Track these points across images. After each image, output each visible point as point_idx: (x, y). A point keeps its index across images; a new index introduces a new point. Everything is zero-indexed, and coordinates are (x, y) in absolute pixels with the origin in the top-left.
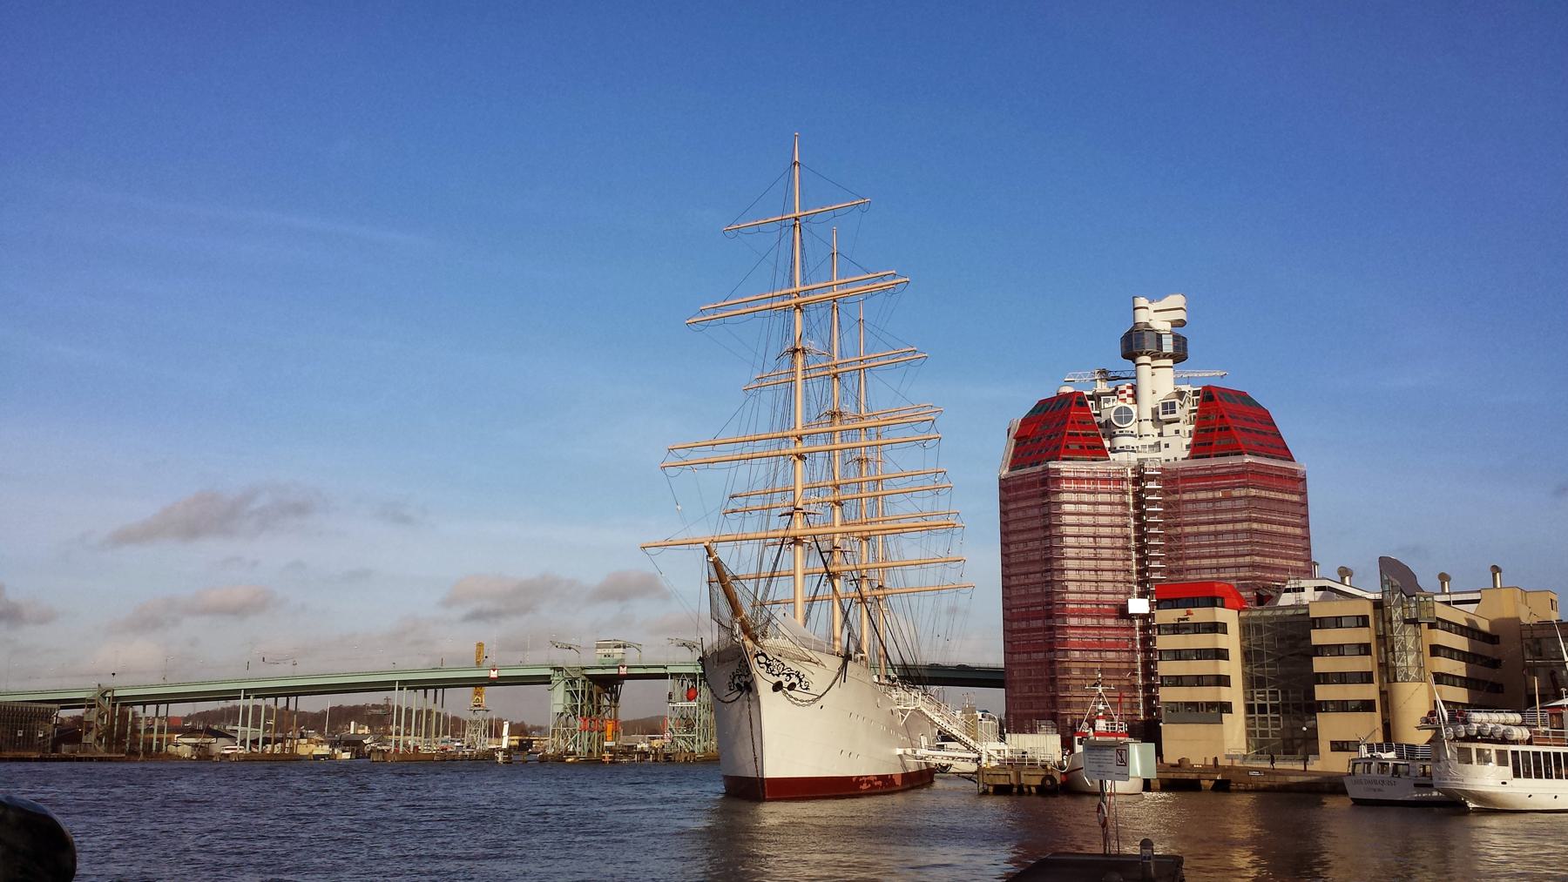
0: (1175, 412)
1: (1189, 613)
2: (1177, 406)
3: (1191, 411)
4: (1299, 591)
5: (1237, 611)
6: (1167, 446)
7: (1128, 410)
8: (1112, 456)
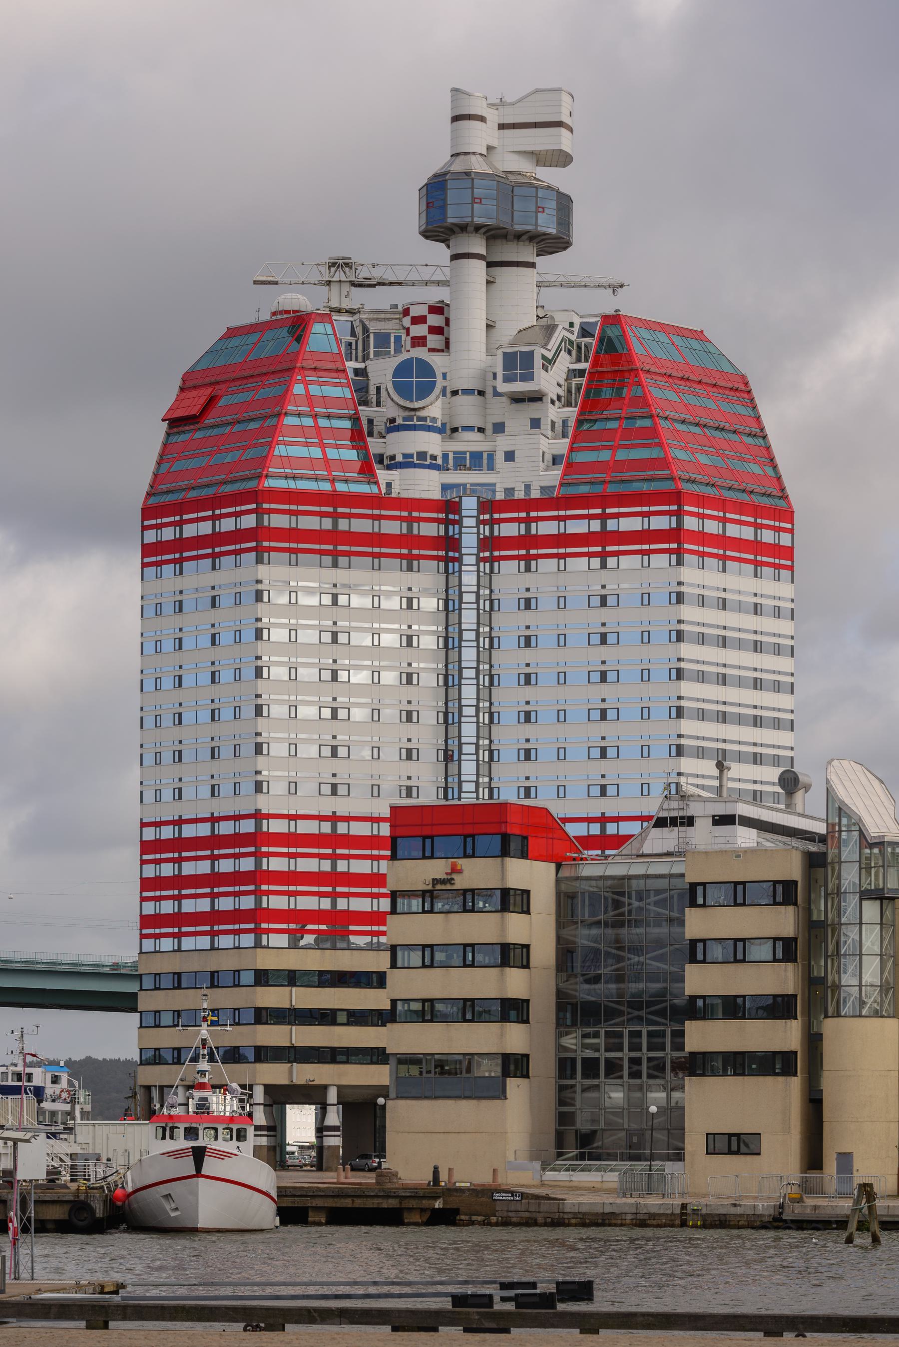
0: (529, 377)
1: (455, 870)
2: (538, 362)
3: (572, 374)
4: (682, 824)
5: (553, 866)
6: (510, 456)
7: (426, 369)
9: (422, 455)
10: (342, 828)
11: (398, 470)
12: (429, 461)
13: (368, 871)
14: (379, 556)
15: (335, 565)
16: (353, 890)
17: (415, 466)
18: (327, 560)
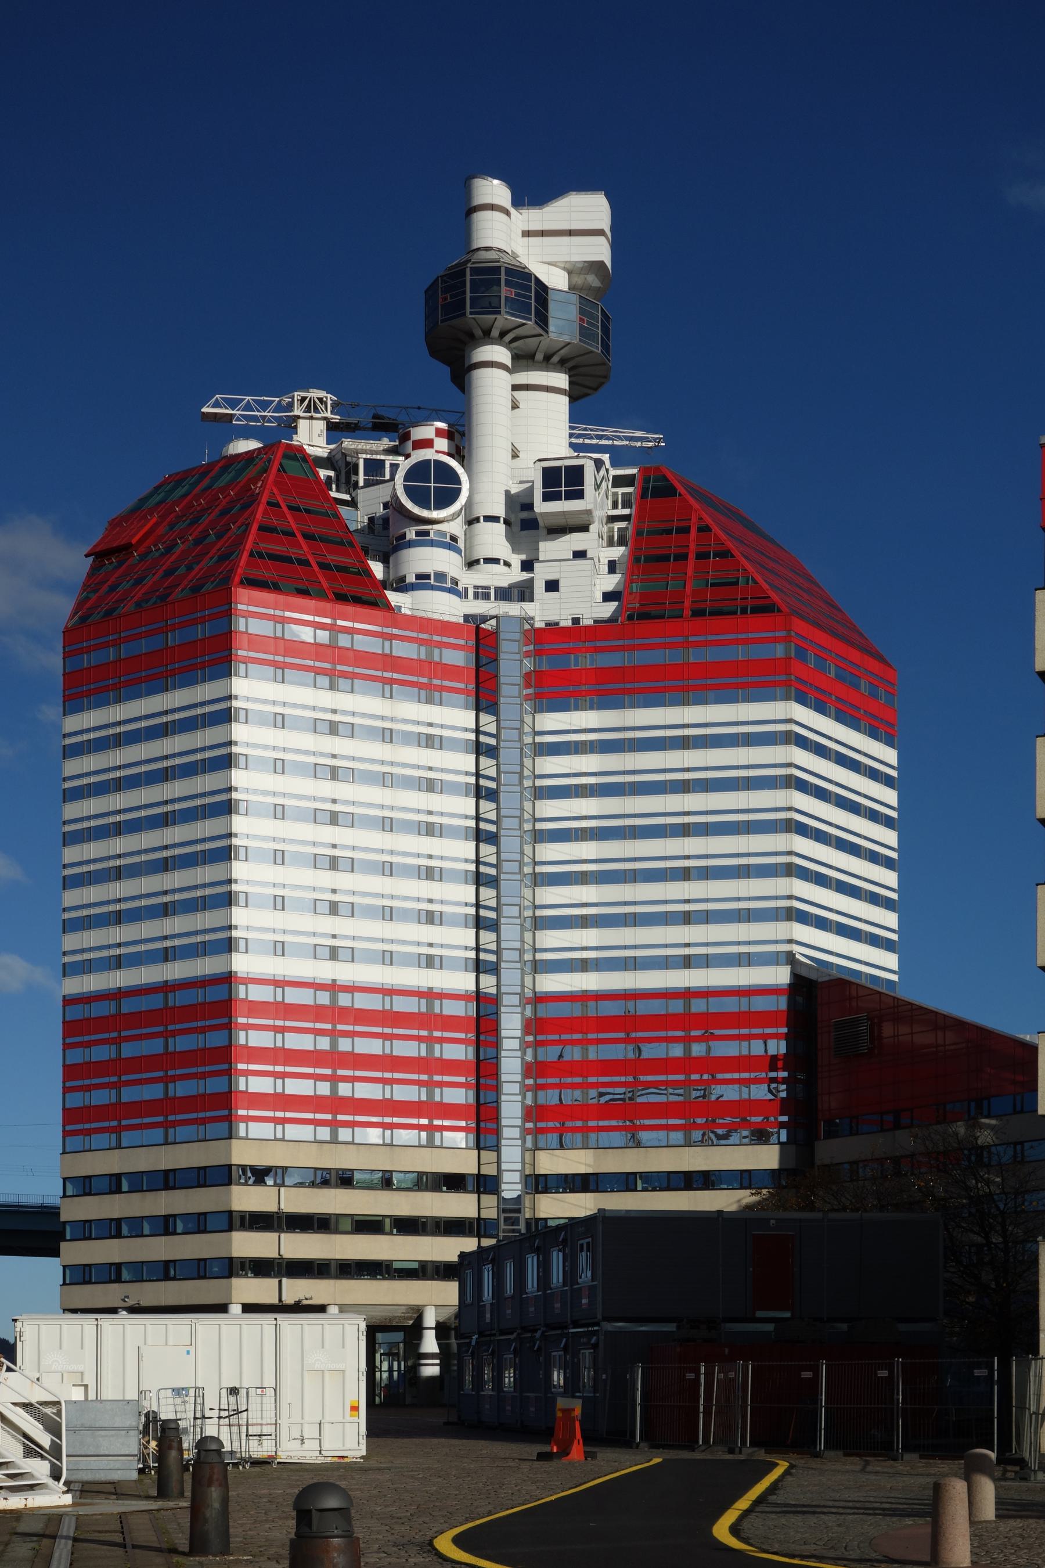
6: (552, 586)
8: (394, 597)
9: (441, 576)
10: (344, 1000)
11: (410, 593)
12: (449, 585)
13: (378, 1051)
14: (391, 682)
16: (358, 1073)
17: (432, 588)
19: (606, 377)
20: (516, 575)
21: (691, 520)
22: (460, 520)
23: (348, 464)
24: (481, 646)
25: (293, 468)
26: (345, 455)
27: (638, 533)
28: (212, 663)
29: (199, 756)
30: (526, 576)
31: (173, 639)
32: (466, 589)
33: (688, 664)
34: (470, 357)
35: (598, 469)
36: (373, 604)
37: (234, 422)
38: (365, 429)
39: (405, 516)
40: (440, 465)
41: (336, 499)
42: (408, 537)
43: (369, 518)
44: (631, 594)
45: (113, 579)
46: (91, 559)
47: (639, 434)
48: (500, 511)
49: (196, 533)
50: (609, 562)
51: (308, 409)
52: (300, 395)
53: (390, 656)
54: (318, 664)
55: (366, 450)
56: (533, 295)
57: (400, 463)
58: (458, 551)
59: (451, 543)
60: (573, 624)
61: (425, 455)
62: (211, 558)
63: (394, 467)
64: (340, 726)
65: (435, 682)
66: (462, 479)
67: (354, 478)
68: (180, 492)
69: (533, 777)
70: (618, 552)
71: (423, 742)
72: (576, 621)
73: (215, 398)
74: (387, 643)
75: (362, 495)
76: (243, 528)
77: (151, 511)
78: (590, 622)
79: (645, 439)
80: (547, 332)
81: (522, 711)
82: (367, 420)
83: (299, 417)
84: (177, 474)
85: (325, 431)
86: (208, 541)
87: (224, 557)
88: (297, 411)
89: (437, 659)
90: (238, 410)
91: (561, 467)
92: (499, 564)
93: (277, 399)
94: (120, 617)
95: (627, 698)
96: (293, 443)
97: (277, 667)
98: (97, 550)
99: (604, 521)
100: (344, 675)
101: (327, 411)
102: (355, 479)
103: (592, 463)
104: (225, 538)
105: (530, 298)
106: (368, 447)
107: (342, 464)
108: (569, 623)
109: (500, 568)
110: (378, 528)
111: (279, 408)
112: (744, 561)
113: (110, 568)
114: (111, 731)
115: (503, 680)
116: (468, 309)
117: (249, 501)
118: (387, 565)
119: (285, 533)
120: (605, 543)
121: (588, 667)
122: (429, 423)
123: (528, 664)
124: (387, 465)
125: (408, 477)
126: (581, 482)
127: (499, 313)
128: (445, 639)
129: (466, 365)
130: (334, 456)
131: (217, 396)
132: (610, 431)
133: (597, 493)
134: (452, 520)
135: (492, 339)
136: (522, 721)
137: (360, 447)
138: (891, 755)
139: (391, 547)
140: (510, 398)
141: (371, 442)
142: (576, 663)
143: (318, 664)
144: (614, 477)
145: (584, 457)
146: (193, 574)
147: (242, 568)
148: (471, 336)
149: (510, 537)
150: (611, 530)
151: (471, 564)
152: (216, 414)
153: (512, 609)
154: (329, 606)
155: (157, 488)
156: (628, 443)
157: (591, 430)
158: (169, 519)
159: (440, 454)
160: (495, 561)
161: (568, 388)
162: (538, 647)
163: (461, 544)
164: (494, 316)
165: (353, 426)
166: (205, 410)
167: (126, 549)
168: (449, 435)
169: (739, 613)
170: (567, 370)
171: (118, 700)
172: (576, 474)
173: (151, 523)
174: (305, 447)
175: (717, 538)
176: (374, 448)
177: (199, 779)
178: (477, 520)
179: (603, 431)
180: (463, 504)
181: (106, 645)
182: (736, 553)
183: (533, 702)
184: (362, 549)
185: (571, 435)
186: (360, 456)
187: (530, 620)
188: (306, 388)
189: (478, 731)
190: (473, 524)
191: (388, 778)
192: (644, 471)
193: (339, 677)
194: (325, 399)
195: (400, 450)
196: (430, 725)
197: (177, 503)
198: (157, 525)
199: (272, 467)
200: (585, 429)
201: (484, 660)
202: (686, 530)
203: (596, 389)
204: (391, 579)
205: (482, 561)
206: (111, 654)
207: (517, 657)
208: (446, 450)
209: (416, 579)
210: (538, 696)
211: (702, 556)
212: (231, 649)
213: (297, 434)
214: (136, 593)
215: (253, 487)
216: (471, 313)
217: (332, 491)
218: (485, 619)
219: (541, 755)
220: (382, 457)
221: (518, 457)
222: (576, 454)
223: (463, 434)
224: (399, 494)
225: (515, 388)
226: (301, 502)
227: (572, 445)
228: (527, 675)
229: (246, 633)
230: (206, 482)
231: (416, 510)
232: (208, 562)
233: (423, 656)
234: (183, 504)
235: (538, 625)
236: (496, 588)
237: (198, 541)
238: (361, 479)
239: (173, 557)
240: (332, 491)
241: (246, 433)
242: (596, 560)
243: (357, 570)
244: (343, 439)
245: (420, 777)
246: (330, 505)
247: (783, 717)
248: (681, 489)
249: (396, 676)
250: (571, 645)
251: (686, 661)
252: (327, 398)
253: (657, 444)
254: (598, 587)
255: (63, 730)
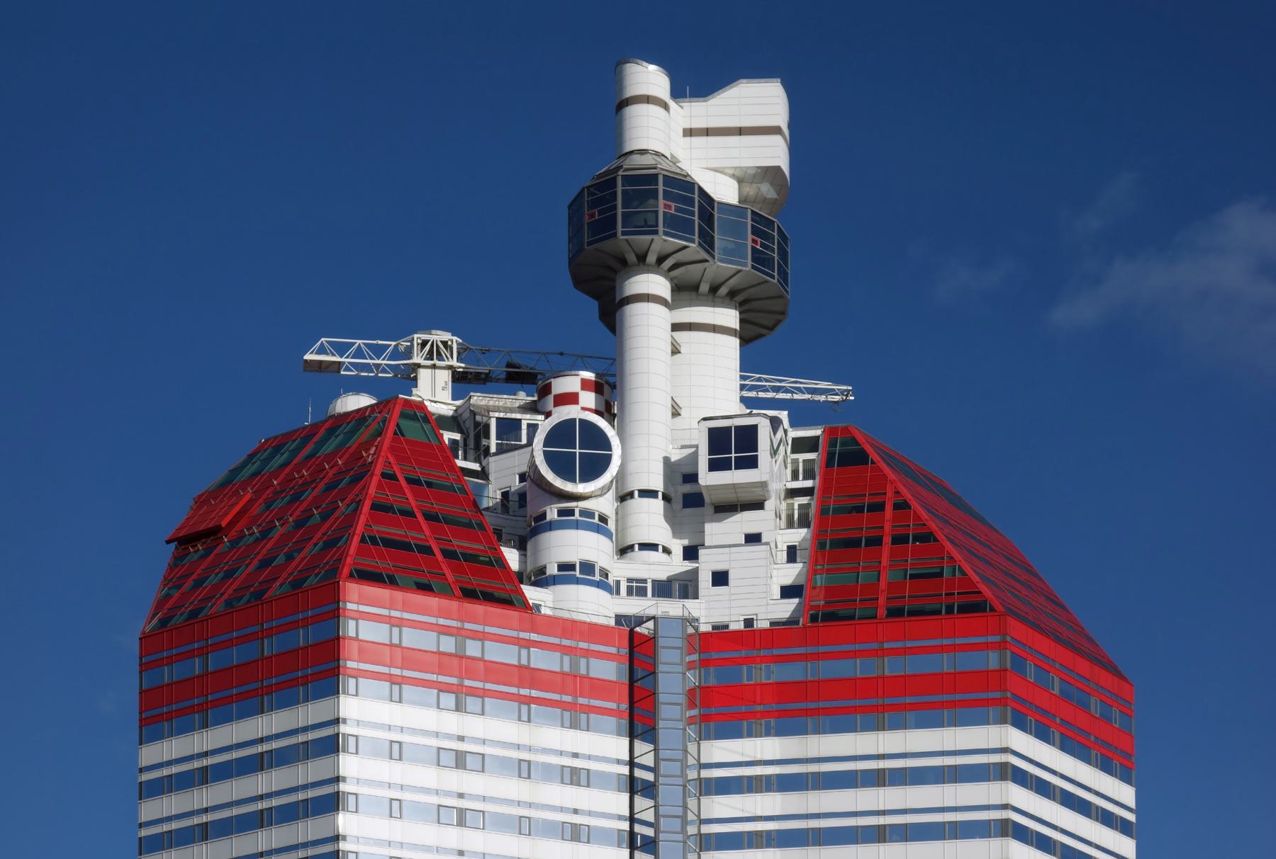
8: (532, 593)
9: (588, 567)
11: (552, 588)
12: (597, 578)
14: (529, 701)
15: (459, 708)
17: (578, 581)
18: (448, 699)
19: (783, 313)
20: (676, 565)
21: (885, 494)
22: (611, 495)
23: (477, 424)
24: (636, 655)
25: (413, 431)
26: (474, 414)
27: (823, 512)
28: (317, 676)
29: (301, 796)
30: (689, 566)
31: (271, 647)
32: (618, 583)
33: (883, 678)
34: (622, 288)
35: (775, 430)
36: (506, 602)
37: (342, 373)
38: (498, 380)
39: (545, 490)
40: (587, 426)
41: (463, 469)
42: (549, 518)
43: (502, 493)
44: (814, 588)
45: (199, 571)
46: (173, 545)
47: (823, 385)
48: (657, 484)
49: (298, 513)
50: (789, 547)
51: (430, 356)
52: (420, 338)
53: (527, 668)
54: (442, 679)
55: (498, 407)
56: (696, 210)
57: (540, 423)
58: (608, 534)
59: (599, 525)
60: (745, 627)
61: (569, 413)
62: (316, 544)
63: (533, 428)
64: (469, 757)
65: (581, 700)
66: (612, 444)
67: (484, 442)
68: (279, 460)
69: (698, 822)
70: (799, 535)
71: (567, 779)
72: (749, 622)
73: (320, 341)
74: (524, 652)
75: (494, 464)
76: (354, 505)
77: (244, 485)
78: (766, 625)
79: (832, 392)
80: (713, 257)
81: (685, 739)
82: (500, 370)
83: (419, 366)
84: (275, 438)
85: (450, 383)
86: (311, 522)
87: (331, 544)
88: (417, 359)
89: (583, 671)
90: (347, 357)
91: (731, 427)
92: (657, 550)
93: (393, 343)
94: (207, 620)
95: (810, 721)
96: (413, 398)
97: (393, 683)
98: (181, 535)
99: (782, 496)
100: (473, 692)
101: (452, 358)
102: (486, 444)
103: (767, 422)
104: (331, 520)
105: (693, 214)
106: (501, 404)
107: (469, 425)
108: (741, 626)
109: (658, 556)
110: (513, 505)
111: (396, 355)
112: (948, 546)
113: (196, 557)
114: (197, 764)
115: (662, 698)
116: (620, 228)
117: (361, 472)
118: (522, 552)
119: (403, 513)
120: (783, 523)
121: (764, 681)
122: (573, 372)
123: (693, 678)
124: (524, 427)
125: (548, 442)
126: (754, 448)
127: (656, 232)
128: (594, 647)
129: (618, 299)
130: (461, 415)
131: (323, 339)
132: (788, 382)
133: (774, 460)
134: (600, 495)
135: (649, 265)
136: (686, 751)
137: (491, 403)
138: (1126, 794)
139: (529, 529)
140: (669, 340)
141: (505, 396)
142: (750, 677)
143: (442, 679)
144: (794, 440)
145: (758, 415)
146: (293, 565)
147: (352, 558)
148: (624, 262)
149: (670, 517)
150: (790, 507)
151: (624, 551)
152: (321, 362)
153: (672, 608)
154: (454, 604)
155: (252, 456)
156: (810, 396)
157: (767, 381)
158: (265, 496)
159: (587, 412)
160: (652, 547)
161: (738, 328)
162: (704, 656)
163: (611, 525)
164: (649, 237)
165: (483, 376)
166: (308, 357)
167: (213, 533)
168: (597, 387)
169: (943, 613)
170: (737, 305)
171: (205, 725)
172: (748, 437)
173: (246, 499)
174: (427, 403)
175: (917, 517)
176: (509, 405)
177: (301, 825)
178: (631, 495)
179: (781, 381)
180: (614, 475)
181: (190, 655)
182: (940, 536)
183: (698, 726)
184: (494, 533)
185: (742, 387)
186: (491, 414)
187: (693, 621)
188: (427, 329)
189: (632, 764)
190: (626, 553)
191: (525, 824)
192: (830, 432)
193: (466, 695)
194: (450, 343)
195: (539, 407)
196: (576, 755)
197: (275, 474)
198: (251, 502)
199: (387, 429)
200: (759, 380)
201: (639, 673)
202: (880, 507)
203: (771, 329)
204: (528, 570)
205: (637, 547)
206: (196, 666)
207: (679, 669)
208: (593, 407)
209: (559, 570)
210: (705, 718)
211: (899, 540)
212: (338, 660)
213: (416, 387)
214: (227, 589)
215: (364, 454)
216: (624, 233)
217: (458, 458)
218: (640, 620)
219: (708, 793)
220: (518, 416)
221: (680, 415)
222: (748, 411)
223: (613, 387)
224: (538, 463)
225: (676, 327)
226: (422, 474)
227: (744, 400)
228: (691, 693)
229: (356, 639)
230: (308, 450)
231: (559, 483)
232: (311, 550)
233: (566, 669)
234: (282, 476)
235: (705, 628)
236: (653, 581)
237: (300, 524)
238: (493, 443)
239: (270, 545)
240: (458, 458)
241: (357, 386)
242: (773, 545)
243: (488, 559)
244: (472, 394)
245: (563, 823)
246: (455, 477)
247: (998, 746)
248: (873, 455)
249: (534, 693)
250: (744, 653)
251: (880, 674)
252: (452, 341)
253: (844, 398)
254: (775, 579)
255: (140, 764)
